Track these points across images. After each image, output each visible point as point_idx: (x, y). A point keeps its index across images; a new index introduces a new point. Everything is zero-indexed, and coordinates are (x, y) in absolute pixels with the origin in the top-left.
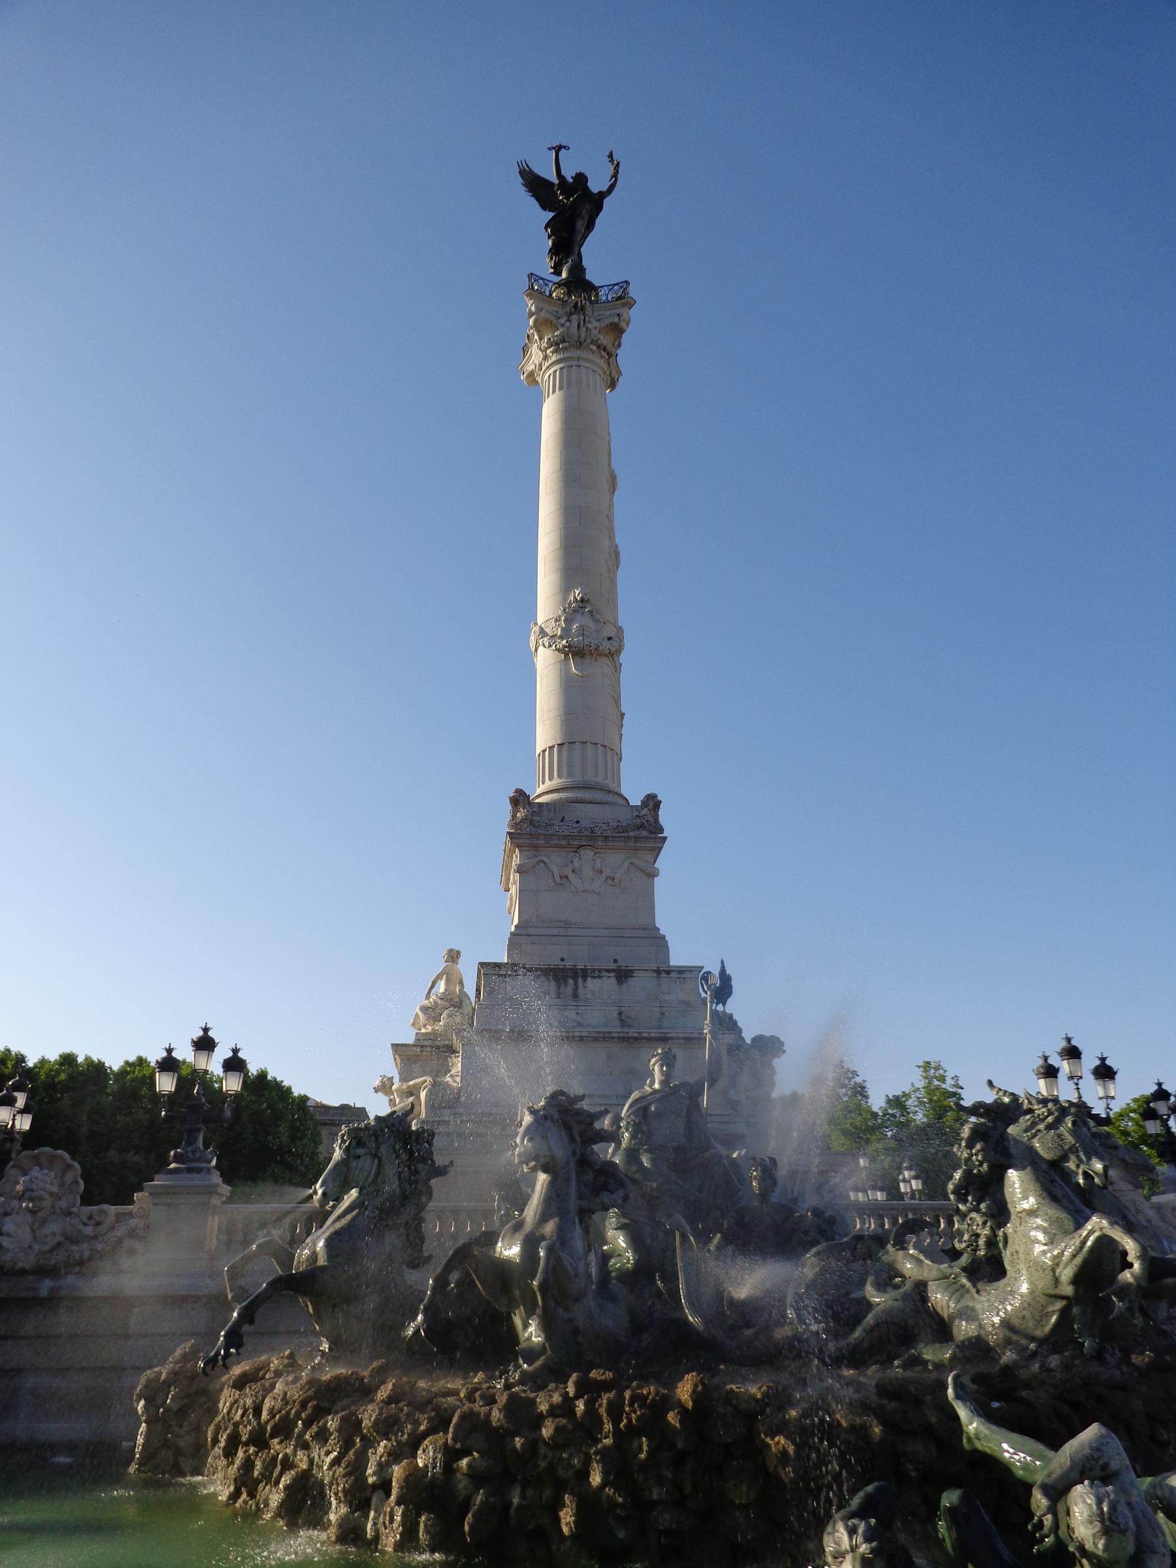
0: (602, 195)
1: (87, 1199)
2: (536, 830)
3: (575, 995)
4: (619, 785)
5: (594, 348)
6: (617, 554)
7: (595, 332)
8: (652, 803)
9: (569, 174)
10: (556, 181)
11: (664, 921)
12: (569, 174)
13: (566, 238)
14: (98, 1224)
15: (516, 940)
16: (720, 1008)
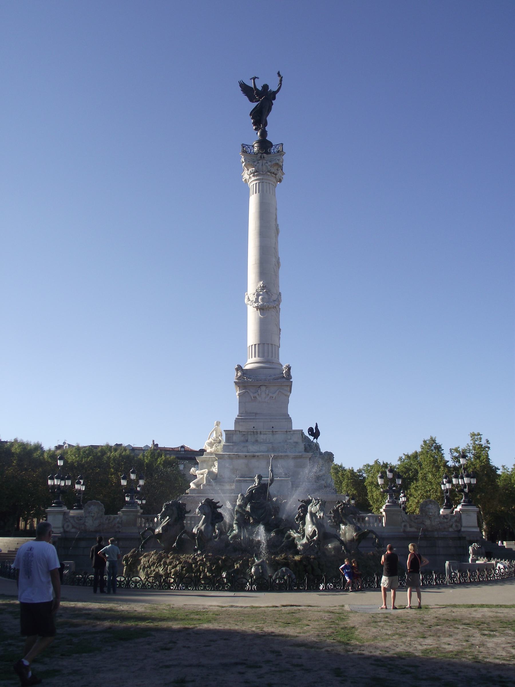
0: (275, 93)
1: (106, 513)
2: (246, 380)
3: (257, 441)
4: (278, 358)
5: (269, 174)
7: (269, 167)
11: (291, 412)
13: (259, 117)
14: (109, 520)
15: (237, 421)
16: (315, 441)
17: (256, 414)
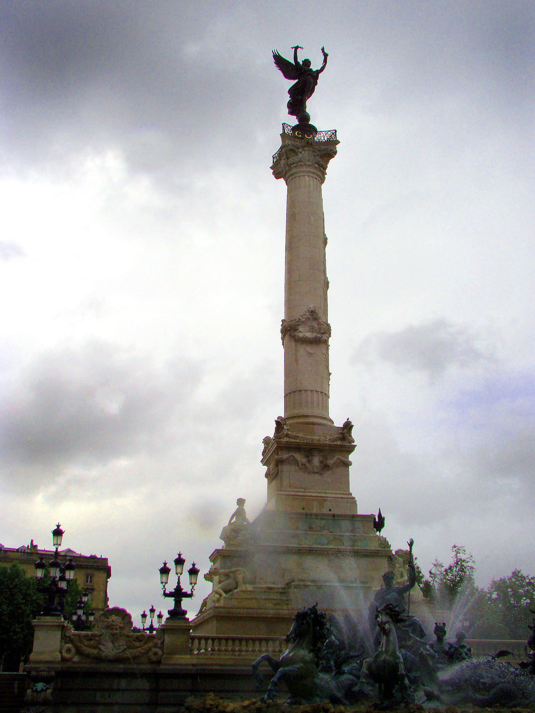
5: (317, 166)
6: (328, 283)
8: (348, 426)
9: (300, 61)
10: (293, 62)
12: (300, 61)
17: (305, 489)
